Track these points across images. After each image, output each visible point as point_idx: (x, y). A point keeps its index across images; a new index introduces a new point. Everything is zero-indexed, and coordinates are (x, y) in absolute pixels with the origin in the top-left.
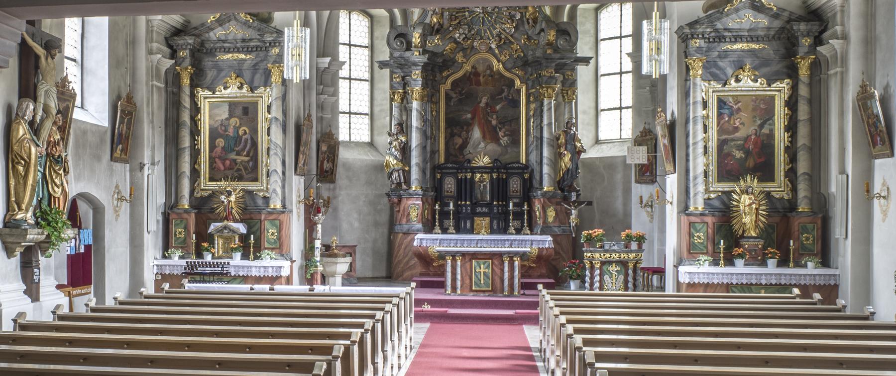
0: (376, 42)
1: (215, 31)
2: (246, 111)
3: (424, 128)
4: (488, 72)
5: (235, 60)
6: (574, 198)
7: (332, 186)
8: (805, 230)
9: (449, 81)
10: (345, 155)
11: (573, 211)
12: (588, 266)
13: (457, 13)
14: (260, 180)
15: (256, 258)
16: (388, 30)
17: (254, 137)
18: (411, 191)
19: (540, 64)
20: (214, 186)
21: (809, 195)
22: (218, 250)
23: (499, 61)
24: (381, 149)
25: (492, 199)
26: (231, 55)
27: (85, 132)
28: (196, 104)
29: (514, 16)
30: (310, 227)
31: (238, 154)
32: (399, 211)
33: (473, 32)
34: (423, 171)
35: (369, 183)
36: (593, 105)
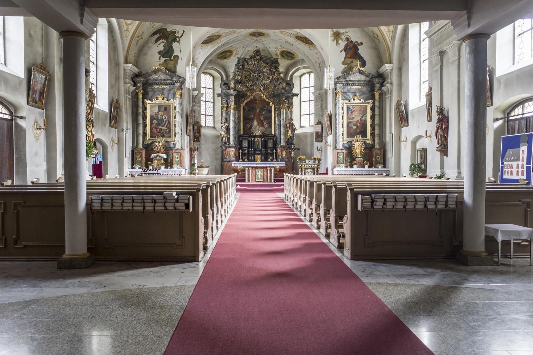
0: (215, 87)
1: (152, 76)
2: (165, 109)
3: (235, 120)
4: (260, 99)
5: (161, 88)
6: (293, 147)
7: (199, 143)
8: (377, 155)
9: (245, 102)
10: (203, 131)
11: (293, 152)
12: (300, 170)
13: (248, 75)
14: (172, 136)
15: (171, 168)
16: (220, 82)
17: (169, 119)
18: (230, 145)
19: (280, 96)
20: (153, 139)
21: (379, 142)
22: (155, 165)
23: (264, 95)
24: (218, 130)
25: (262, 148)
26: (159, 86)
27: (99, 113)
28: (145, 106)
29: (270, 77)
30: (192, 158)
31: (163, 126)
32: (225, 153)
33: (254, 83)
34: (235, 138)
35: (213, 143)
36: (299, 113)
